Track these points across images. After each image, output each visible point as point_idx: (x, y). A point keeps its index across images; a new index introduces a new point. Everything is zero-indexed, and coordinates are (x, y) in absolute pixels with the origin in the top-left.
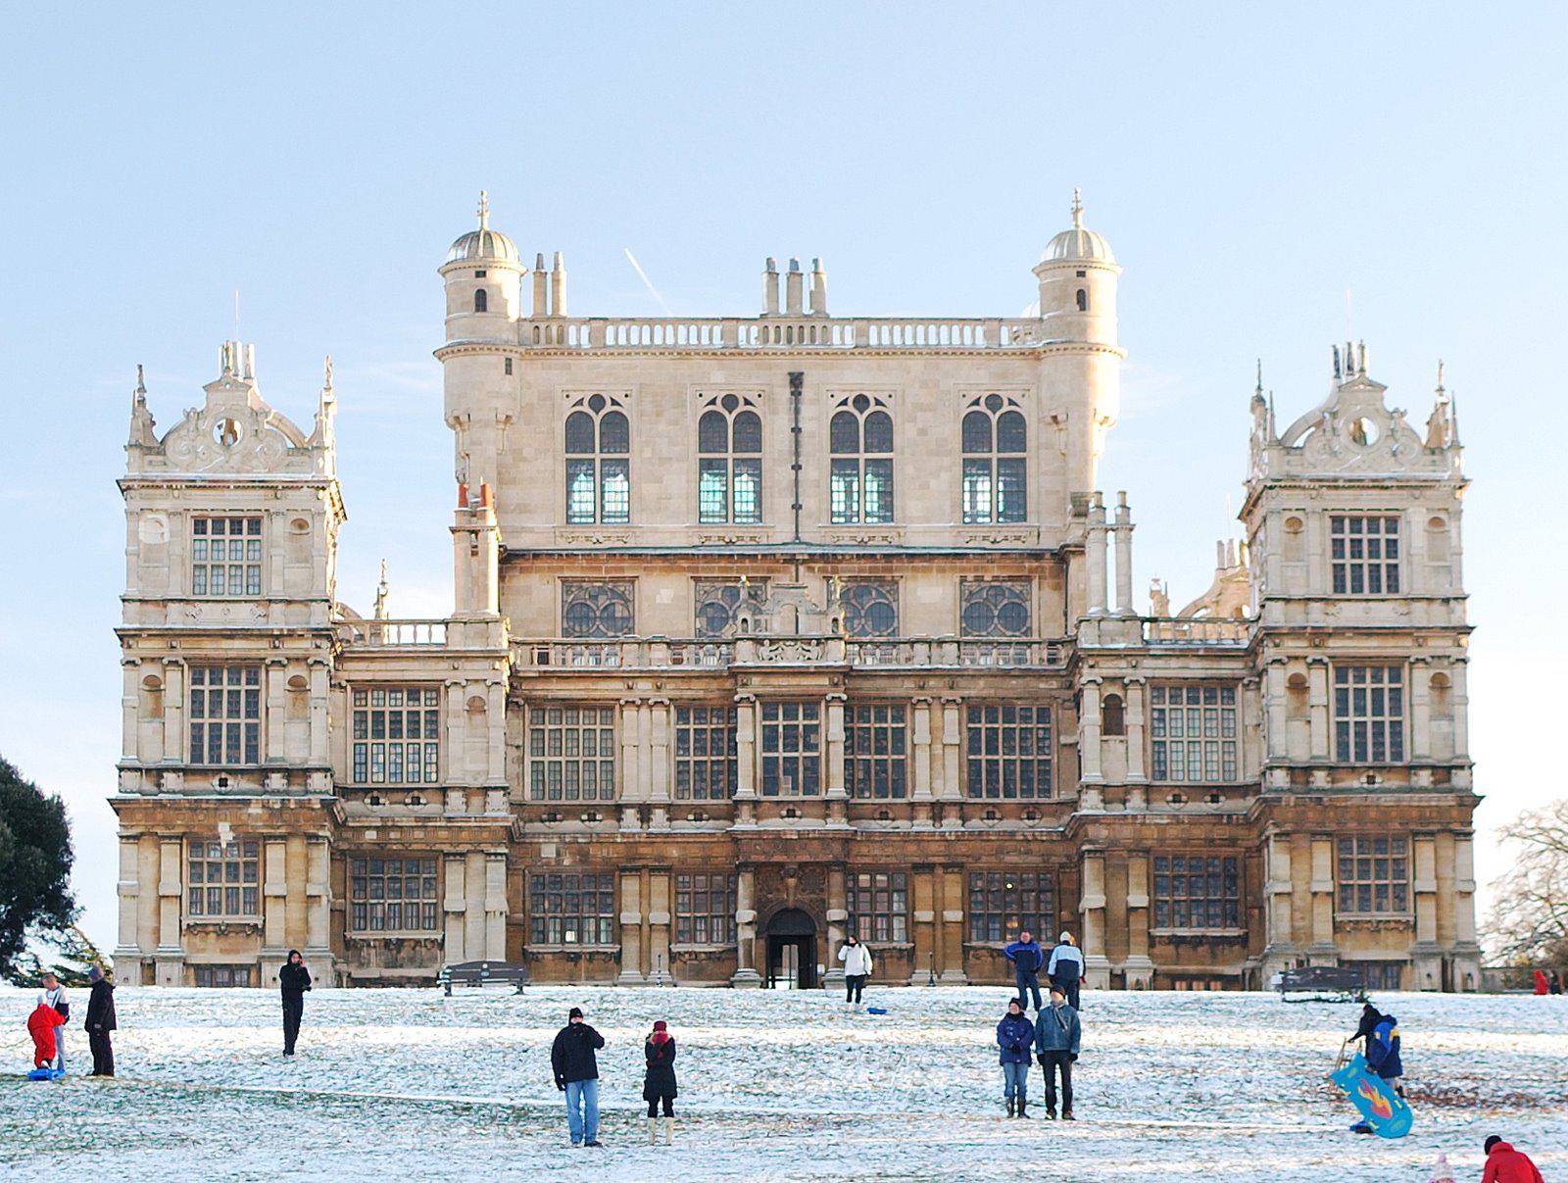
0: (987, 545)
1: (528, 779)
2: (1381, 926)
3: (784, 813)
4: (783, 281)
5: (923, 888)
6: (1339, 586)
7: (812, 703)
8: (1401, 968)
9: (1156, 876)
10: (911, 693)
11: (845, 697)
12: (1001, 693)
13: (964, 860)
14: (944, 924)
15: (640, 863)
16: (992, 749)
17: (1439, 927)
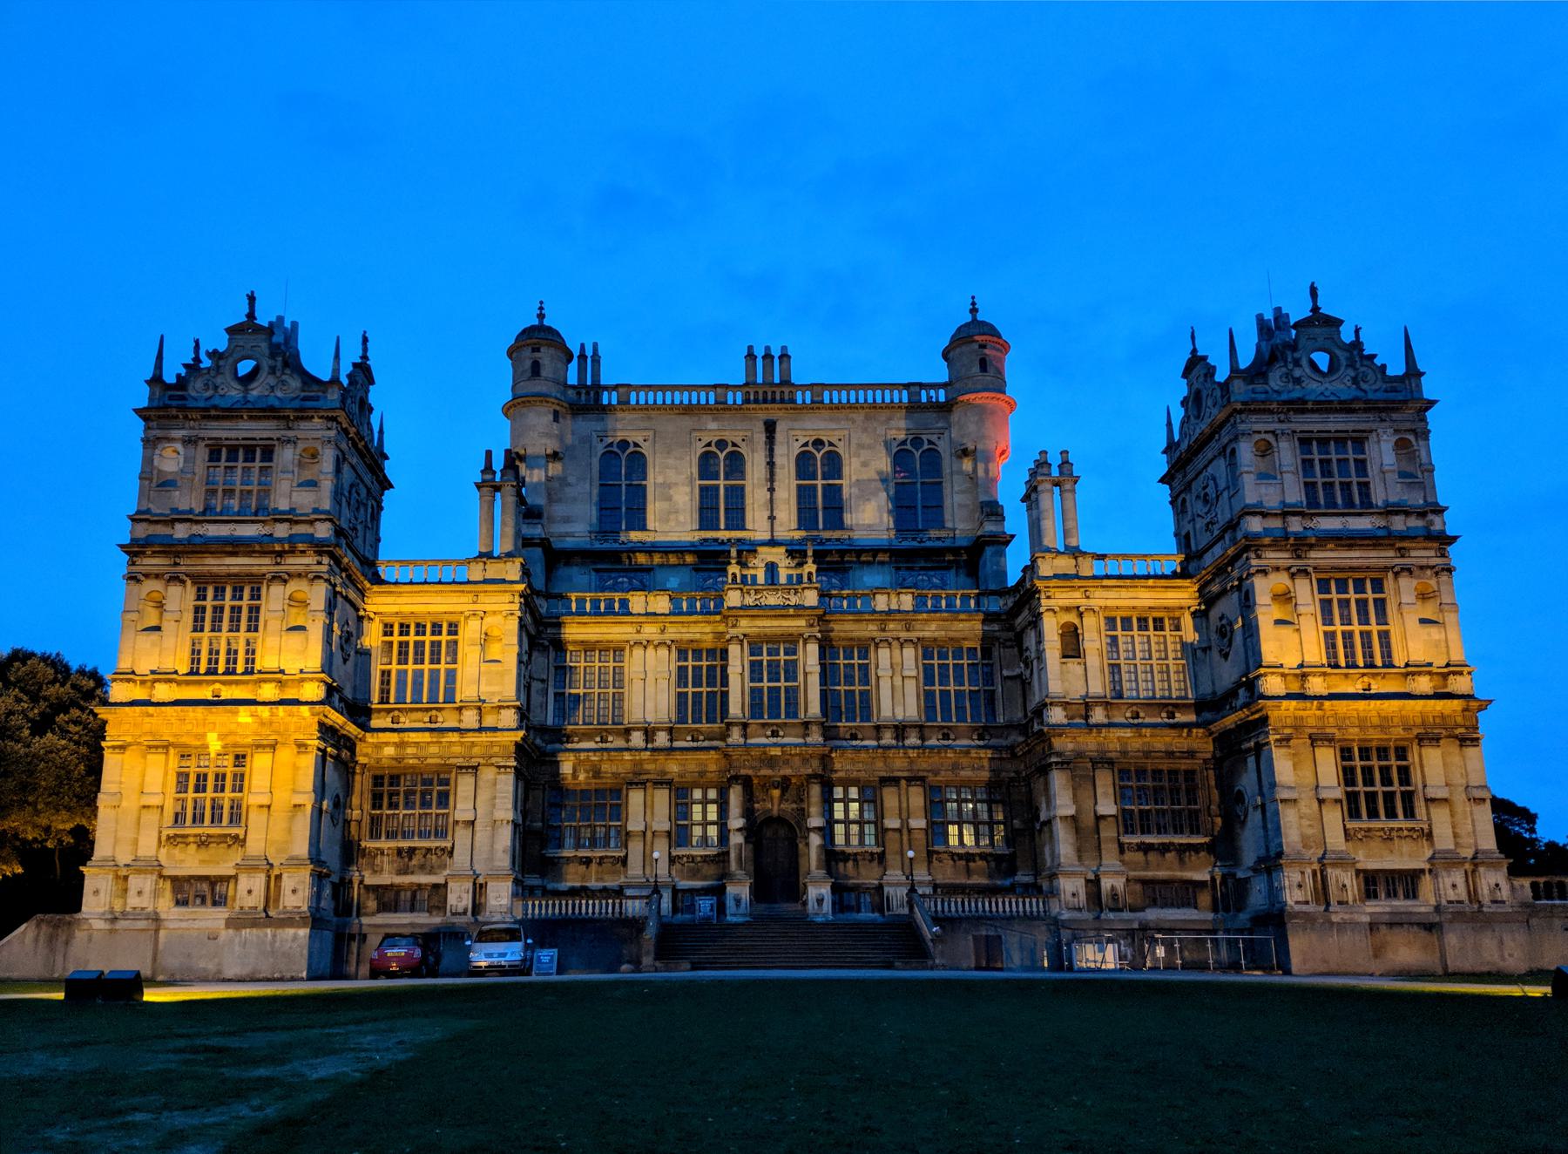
0: (915, 544)
1: (551, 707)
2: (1394, 834)
3: (769, 733)
4: (760, 362)
5: (890, 798)
6: (1312, 502)
7: (792, 642)
8: (1419, 878)
9: (1121, 787)
10: (875, 634)
11: (819, 635)
12: (951, 634)
13: (925, 774)
14: (910, 831)
15: (645, 777)
16: (944, 679)
17: (1455, 835)
